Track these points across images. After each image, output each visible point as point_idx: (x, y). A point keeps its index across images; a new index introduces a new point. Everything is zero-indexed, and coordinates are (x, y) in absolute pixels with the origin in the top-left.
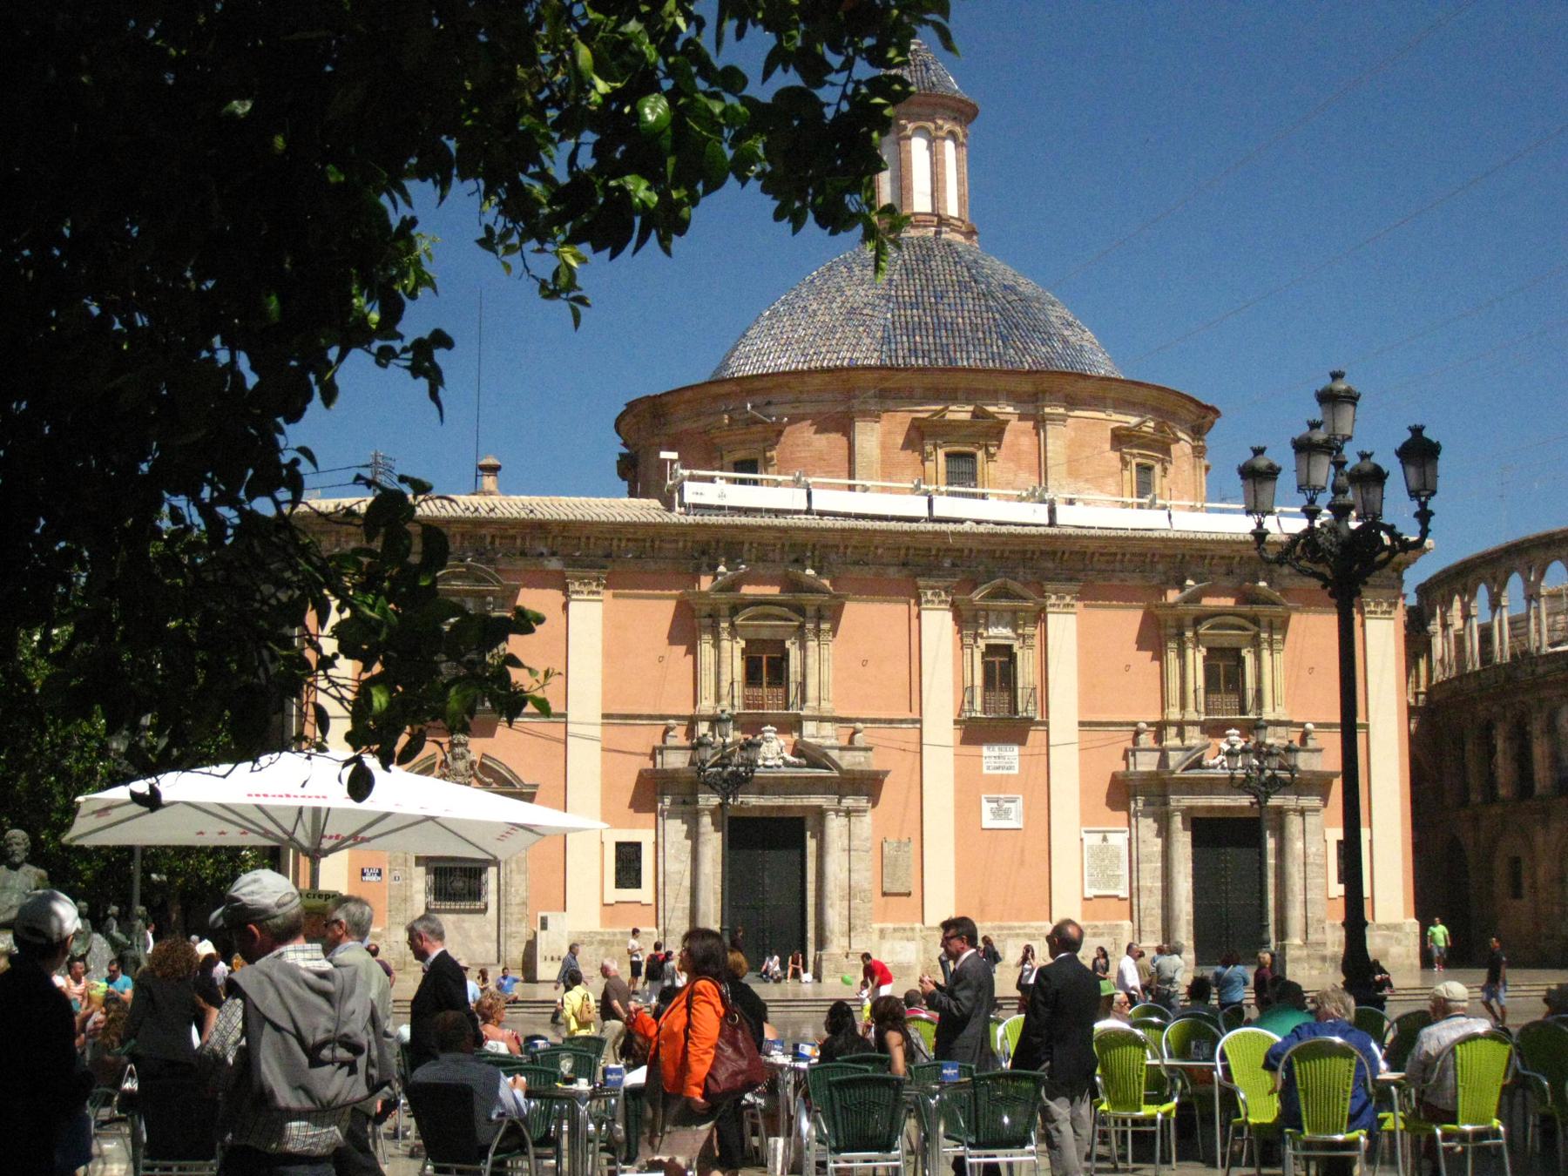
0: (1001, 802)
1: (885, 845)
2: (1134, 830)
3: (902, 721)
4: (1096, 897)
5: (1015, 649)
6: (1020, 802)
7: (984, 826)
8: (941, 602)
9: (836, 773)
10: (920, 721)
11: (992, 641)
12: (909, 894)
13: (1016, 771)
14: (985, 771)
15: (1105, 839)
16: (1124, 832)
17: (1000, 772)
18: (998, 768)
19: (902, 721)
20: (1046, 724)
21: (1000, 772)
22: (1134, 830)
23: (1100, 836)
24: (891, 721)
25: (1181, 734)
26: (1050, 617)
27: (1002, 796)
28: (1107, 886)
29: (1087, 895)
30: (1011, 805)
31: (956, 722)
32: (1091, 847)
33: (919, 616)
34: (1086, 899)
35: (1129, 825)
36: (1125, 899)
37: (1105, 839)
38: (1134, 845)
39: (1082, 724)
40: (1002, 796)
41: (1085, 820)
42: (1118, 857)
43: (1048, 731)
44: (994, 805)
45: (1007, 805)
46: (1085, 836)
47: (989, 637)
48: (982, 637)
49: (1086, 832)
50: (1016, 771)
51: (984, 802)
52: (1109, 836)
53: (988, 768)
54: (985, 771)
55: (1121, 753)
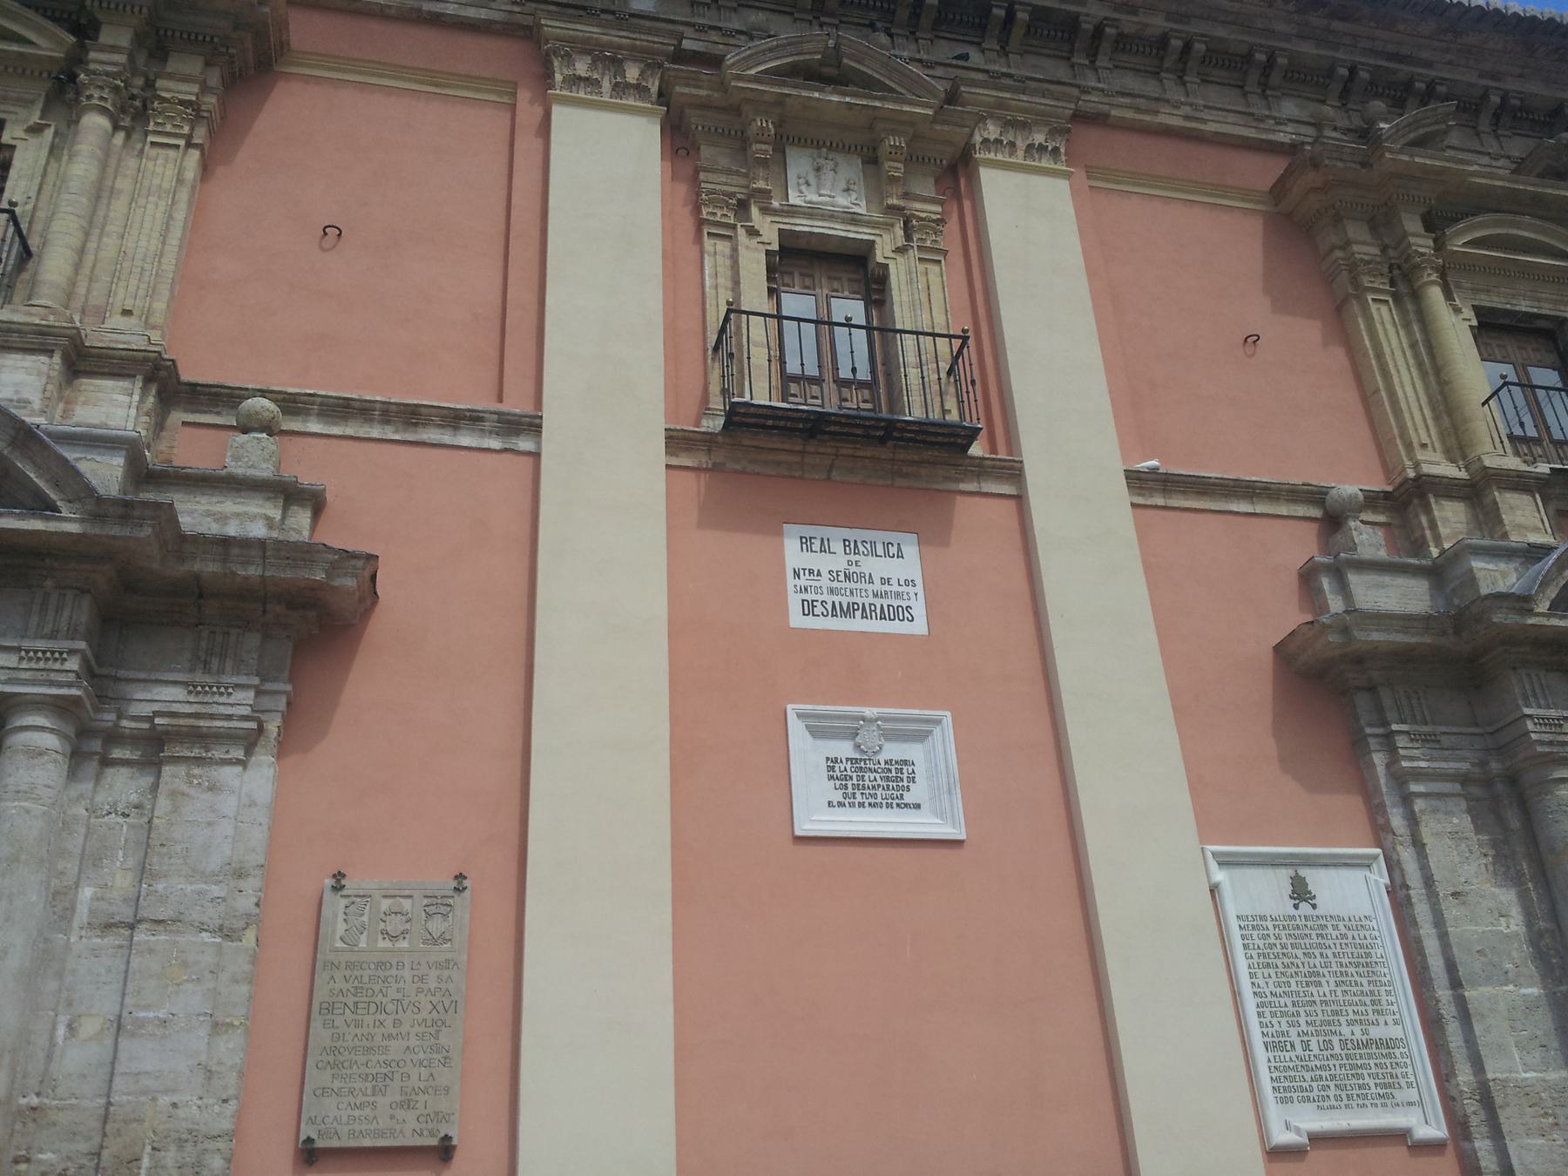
0: (869, 737)
1: (335, 906)
2: (1407, 855)
3: (455, 419)
4: (1317, 1139)
5: (883, 250)
6: (944, 738)
7: (804, 827)
8: (620, 88)
9: (69, 523)
10: (532, 426)
11: (802, 225)
12: (445, 1151)
13: (919, 627)
14: (797, 620)
15: (1300, 892)
16: (1364, 863)
17: (857, 624)
18: (849, 611)
19: (455, 419)
20: (1013, 472)
21: (857, 624)
22: (1407, 855)
23: (1283, 876)
24: (412, 416)
25: (1487, 517)
26: (985, 174)
27: (869, 712)
28: (1359, 1098)
29: (1281, 1137)
30: (913, 751)
31: (676, 441)
32: (1253, 923)
33: (545, 129)
34: (1277, 1154)
35: (1379, 832)
36: (1431, 1147)
37: (1300, 892)
38: (1422, 911)
39: (1137, 481)
40: (869, 712)
41: (1208, 828)
42: (1366, 962)
43: (1020, 499)
44: (844, 749)
45: (893, 751)
46: (1219, 876)
47: (792, 211)
48: (766, 210)
49: (1226, 862)
50: (919, 627)
51: (796, 728)
52: (1317, 879)
53: (809, 608)
54: (797, 620)
55: (1291, 581)
